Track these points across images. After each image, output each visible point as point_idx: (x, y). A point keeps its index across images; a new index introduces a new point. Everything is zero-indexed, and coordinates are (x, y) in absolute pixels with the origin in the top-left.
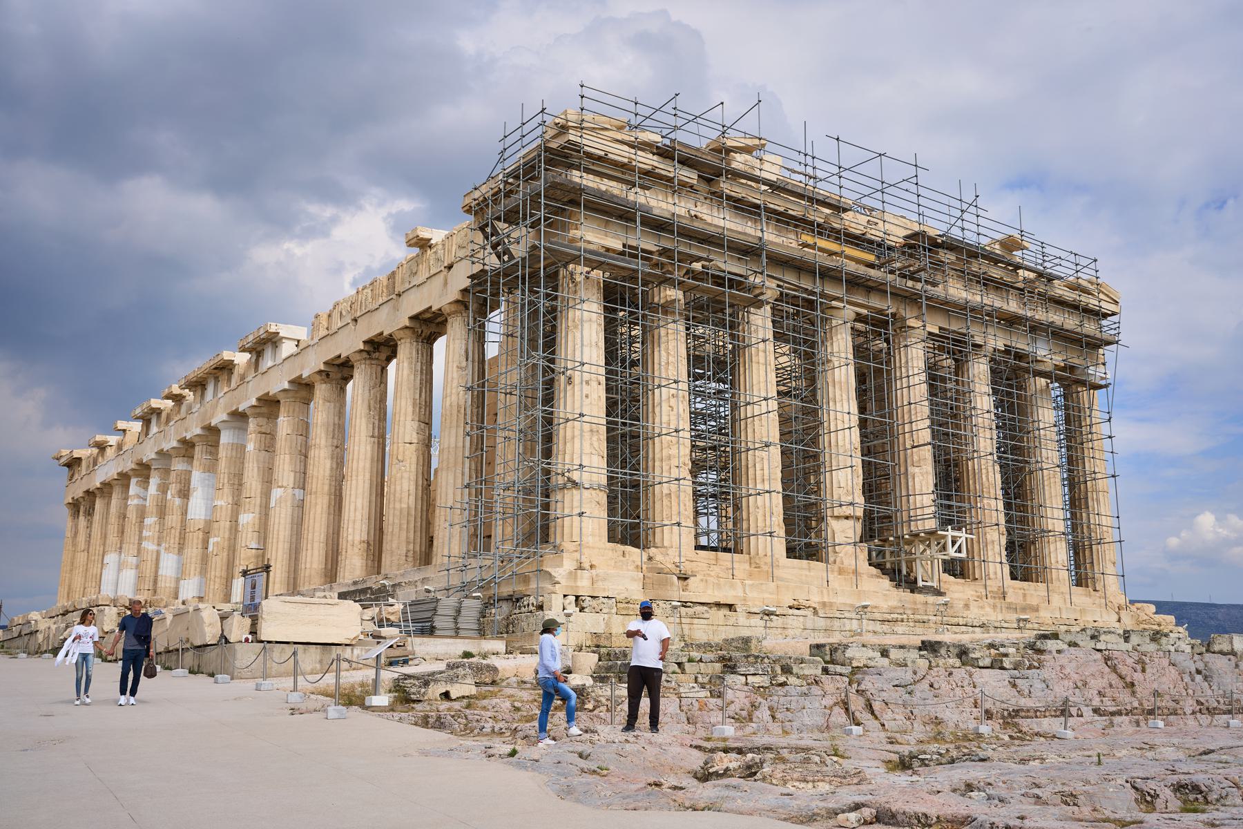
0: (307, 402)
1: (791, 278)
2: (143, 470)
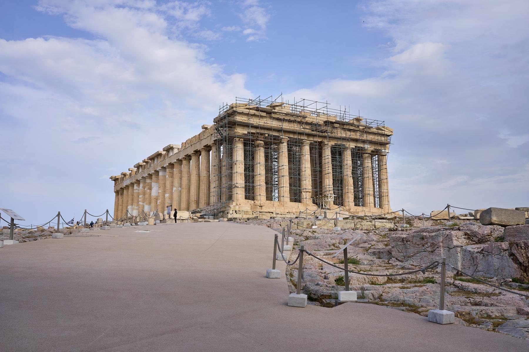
0: (181, 164)
1: (292, 136)
2: (138, 182)
